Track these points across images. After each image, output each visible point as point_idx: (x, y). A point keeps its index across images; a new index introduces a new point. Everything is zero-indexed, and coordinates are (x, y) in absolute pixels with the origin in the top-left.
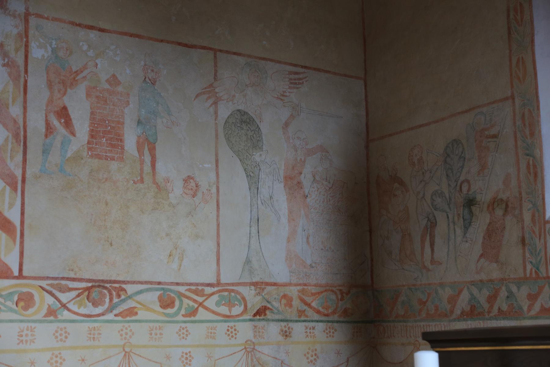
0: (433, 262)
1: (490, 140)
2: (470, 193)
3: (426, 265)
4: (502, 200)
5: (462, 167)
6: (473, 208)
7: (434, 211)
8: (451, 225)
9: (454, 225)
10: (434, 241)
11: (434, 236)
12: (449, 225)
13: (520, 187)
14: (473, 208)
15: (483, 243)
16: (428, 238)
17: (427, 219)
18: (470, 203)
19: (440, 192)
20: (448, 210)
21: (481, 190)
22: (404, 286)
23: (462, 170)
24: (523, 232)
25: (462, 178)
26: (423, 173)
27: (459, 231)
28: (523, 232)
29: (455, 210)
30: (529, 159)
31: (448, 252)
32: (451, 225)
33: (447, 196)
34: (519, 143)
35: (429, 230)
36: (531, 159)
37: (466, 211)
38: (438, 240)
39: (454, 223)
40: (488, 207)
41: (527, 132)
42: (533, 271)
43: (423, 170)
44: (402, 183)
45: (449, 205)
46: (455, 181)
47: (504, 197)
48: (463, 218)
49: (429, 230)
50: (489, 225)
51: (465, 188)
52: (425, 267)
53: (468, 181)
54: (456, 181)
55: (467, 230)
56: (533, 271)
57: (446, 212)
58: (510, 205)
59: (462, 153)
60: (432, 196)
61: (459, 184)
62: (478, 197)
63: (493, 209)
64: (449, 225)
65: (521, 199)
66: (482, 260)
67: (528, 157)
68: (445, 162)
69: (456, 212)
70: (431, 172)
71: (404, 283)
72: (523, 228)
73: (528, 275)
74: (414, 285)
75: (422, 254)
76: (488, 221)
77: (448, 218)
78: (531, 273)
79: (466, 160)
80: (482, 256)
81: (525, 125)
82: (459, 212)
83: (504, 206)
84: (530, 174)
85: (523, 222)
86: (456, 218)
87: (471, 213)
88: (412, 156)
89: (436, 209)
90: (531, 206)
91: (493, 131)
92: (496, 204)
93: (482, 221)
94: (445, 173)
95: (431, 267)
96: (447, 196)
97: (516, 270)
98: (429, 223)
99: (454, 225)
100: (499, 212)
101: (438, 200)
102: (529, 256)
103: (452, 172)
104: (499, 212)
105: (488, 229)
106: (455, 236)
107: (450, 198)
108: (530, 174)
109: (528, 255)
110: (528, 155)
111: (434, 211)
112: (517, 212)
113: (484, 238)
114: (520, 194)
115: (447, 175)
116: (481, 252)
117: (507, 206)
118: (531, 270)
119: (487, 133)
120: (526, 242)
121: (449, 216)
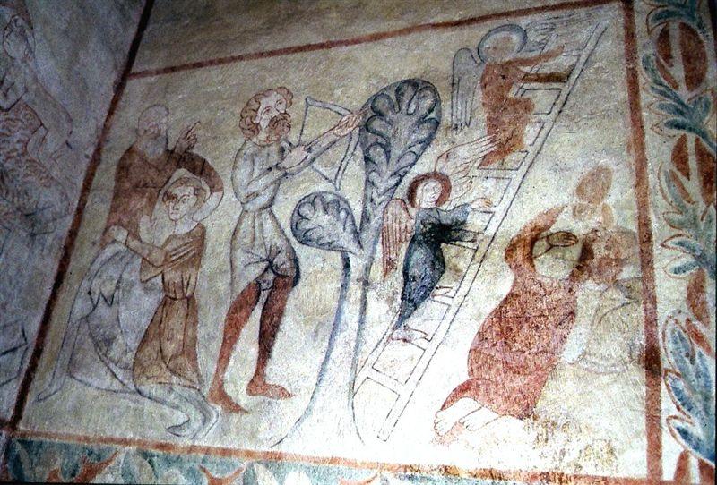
0: (258, 383)
1: (534, 85)
2: (444, 207)
3: (229, 389)
4: (568, 235)
5: (427, 143)
6: (449, 251)
7: (297, 246)
8: (355, 290)
9: (365, 291)
10: (276, 327)
11: (281, 313)
12: (344, 287)
13: (643, 206)
14: (449, 251)
15: (474, 351)
16: (257, 312)
17: (264, 265)
18: (439, 235)
19: (330, 197)
20: (352, 247)
21: (489, 204)
22: (125, 442)
23: (424, 149)
24: (651, 337)
25: (418, 170)
26: (282, 150)
27: (381, 312)
28: (651, 337)
29: (379, 247)
30: (683, 139)
31: (324, 363)
32: (355, 290)
33: (357, 210)
34: (646, 97)
35: (264, 295)
36: (691, 139)
37: (420, 255)
38: (291, 328)
39: (366, 283)
40: (511, 250)
41: (678, 71)
42: (694, 462)
43: (285, 144)
44: (201, 169)
45: (357, 235)
46: (395, 174)
47: (580, 228)
48: (405, 273)
49: (264, 295)
50: (506, 301)
51: (427, 196)
52: (223, 397)
53: (445, 182)
54: (399, 175)
55: (416, 307)
56: (694, 462)
57: (344, 252)
58: (599, 250)
59: (431, 111)
60: (300, 204)
61: (407, 181)
62: (475, 222)
63: (530, 258)
64: (344, 287)
65: (647, 238)
66: (466, 403)
67: (682, 132)
68: (366, 127)
69: (379, 255)
70: (309, 150)
71: (130, 435)
72: (651, 322)
73: (669, 473)
74: (161, 446)
75: (224, 358)
76: (504, 287)
77: (347, 266)
78: (682, 469)
79: (441, 128)
80: (464, 389)
81: (668, 57)
82: (393, 256)
83: (574, 252)
84: (688, 175)
85: (654, 302)
86: (376, 273)
87: (439, 264)
88: (256, 111)
89: (305, 240)
90: (688, 259)
91: (548, 68)
92: (541, 246)
93: (478, 289)
94: (359, 153)
95: (243, 399)
96: (357, 210)
97: (611, 452)
98: (271, 276)
99: (365, 291)
100: (552, 270)
101: (320, 220)
102: (675, 412)
103: (388, 153)
104: (552, 270)
105: (500, 313)
106: (362, 322)
107: (366, 217)
108: (688, 175)
109: (668, 405)
110: (678, 126)
111: (297, 246)
112: (628, 273)
113: (481, 336)
114: (644, 224)
115: (367, 159)
116: (465, 378)
117: (587, 253)
118: (684, 457)
119: (527, 69)
120: (665, 364)
121: (352, 263)
